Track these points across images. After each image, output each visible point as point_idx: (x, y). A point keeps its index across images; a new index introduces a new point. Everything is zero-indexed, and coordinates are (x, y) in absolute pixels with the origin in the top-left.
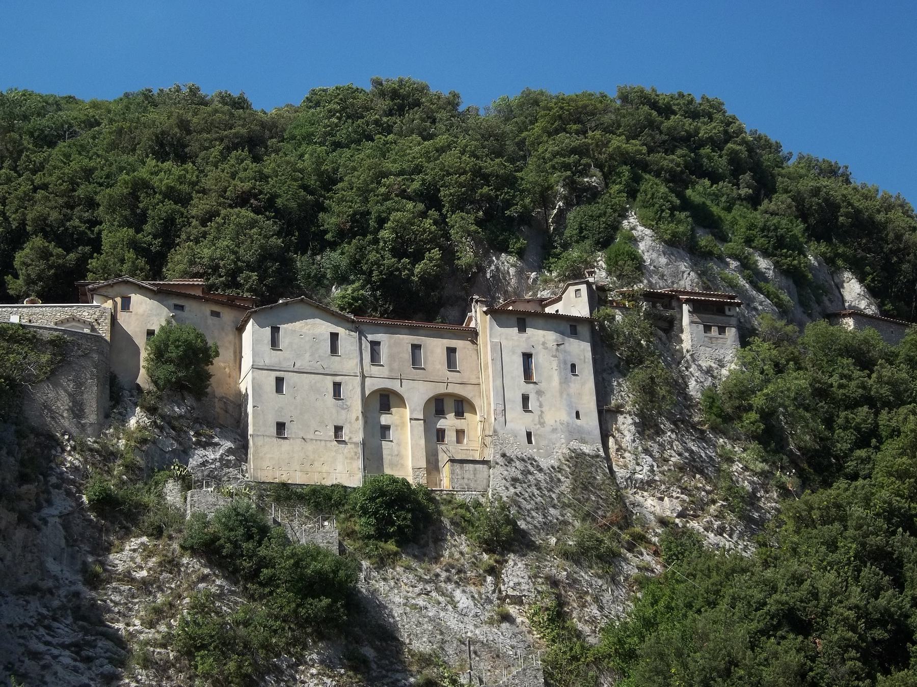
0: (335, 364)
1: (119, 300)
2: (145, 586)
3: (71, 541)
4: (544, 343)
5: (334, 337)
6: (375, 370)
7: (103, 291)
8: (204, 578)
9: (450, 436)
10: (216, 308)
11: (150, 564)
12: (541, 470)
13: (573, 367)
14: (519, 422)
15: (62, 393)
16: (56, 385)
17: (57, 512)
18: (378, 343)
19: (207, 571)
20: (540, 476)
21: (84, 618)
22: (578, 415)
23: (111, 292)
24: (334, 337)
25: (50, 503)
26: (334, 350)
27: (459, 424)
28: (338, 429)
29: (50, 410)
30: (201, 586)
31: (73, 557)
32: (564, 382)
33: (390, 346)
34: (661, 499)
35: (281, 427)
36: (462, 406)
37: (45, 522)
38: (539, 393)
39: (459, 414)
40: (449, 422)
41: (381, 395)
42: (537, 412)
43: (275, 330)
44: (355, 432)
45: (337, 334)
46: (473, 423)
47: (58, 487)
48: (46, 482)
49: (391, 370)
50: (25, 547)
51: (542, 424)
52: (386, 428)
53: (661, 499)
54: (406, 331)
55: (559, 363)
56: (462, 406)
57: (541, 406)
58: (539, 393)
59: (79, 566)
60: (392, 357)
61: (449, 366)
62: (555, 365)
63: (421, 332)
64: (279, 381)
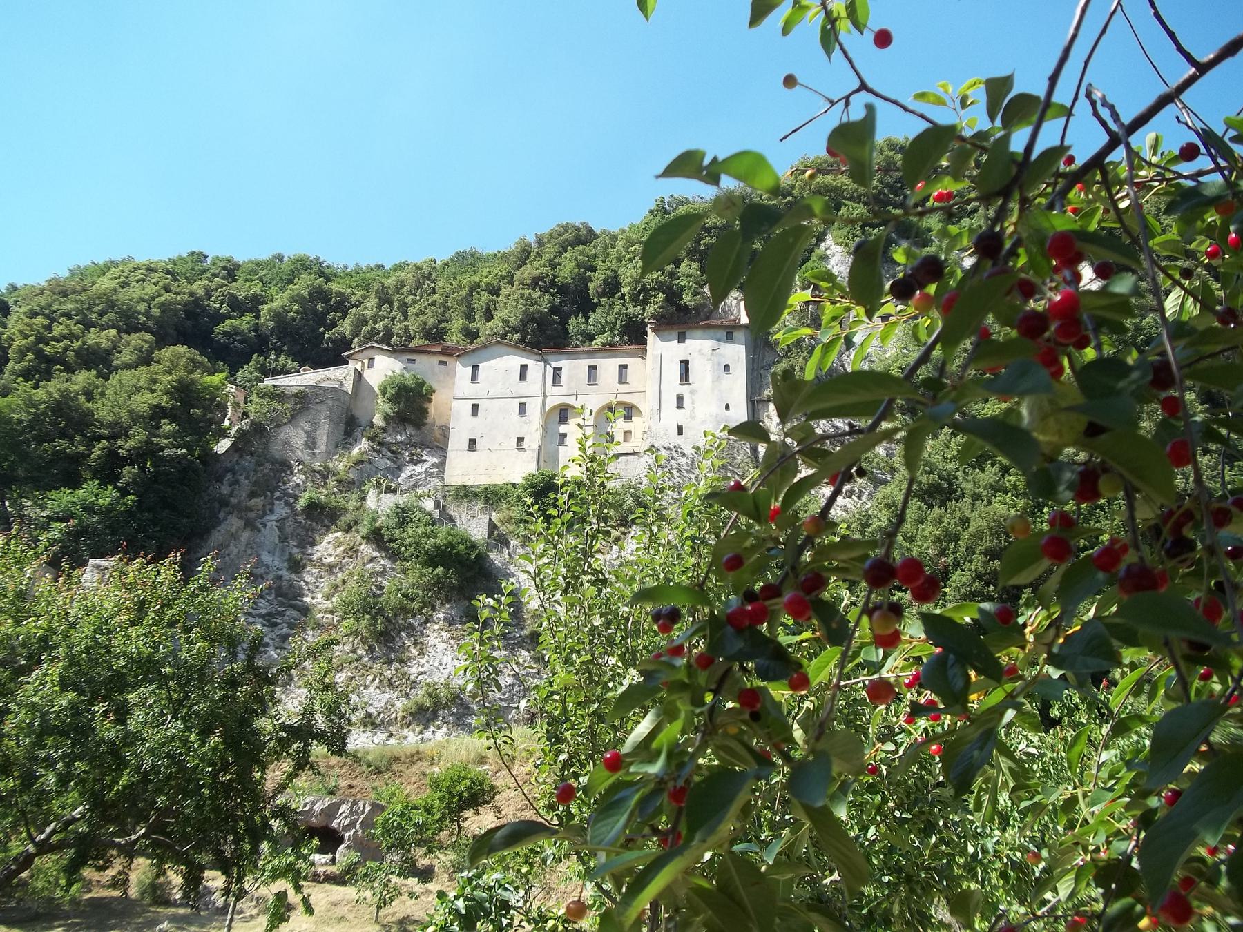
0: (523, 389)
1: (366, 361)
2: (331, 568)
3: (284, 539)
4: (700, 351)
5: (524, 368)
6: (556, 390)
7: (356, 356)
8: (372, 560)
10: (443, 359)
11: (338, 552)
12: (684, 455)
13: (727, 367)
14: (672, 416)
15: (301, 432)
16: (295, 427)
17: (275, 518)
18: (560, 369)
19: (375, 554)
20: (682, 461)
21: (285, 595)
22: (727, 407)
23: (360, 356)
24: (524, 368)
25: (272, 511)
26: (523, 377)
27: (627, 426)
28: (520, 440)
29: (289, 445)
30: (369, 566)
31: (283, 550)
32: (717, 380)
35: (472, 442)
36: (630, 411)
37: (265, 525)
38: (692, 392)
39: (628, 418)
41: (561, 410)
43: (475, 368)
44: (534, 440)
45: (526, 366)
46: (637, 424)
47: (279, 499)
48: (272, 496)
49: (569, 389)
51: (693, 418)
52: (565, 435)
54: (585, 356)
55: (713, 365)
56: (630, 411)
57: (693, 403)
58: (692, 392)
59: (287, 556)
61: (620, 379)
62: (709, 365)
63: (598, 355)
64: (475, 408)
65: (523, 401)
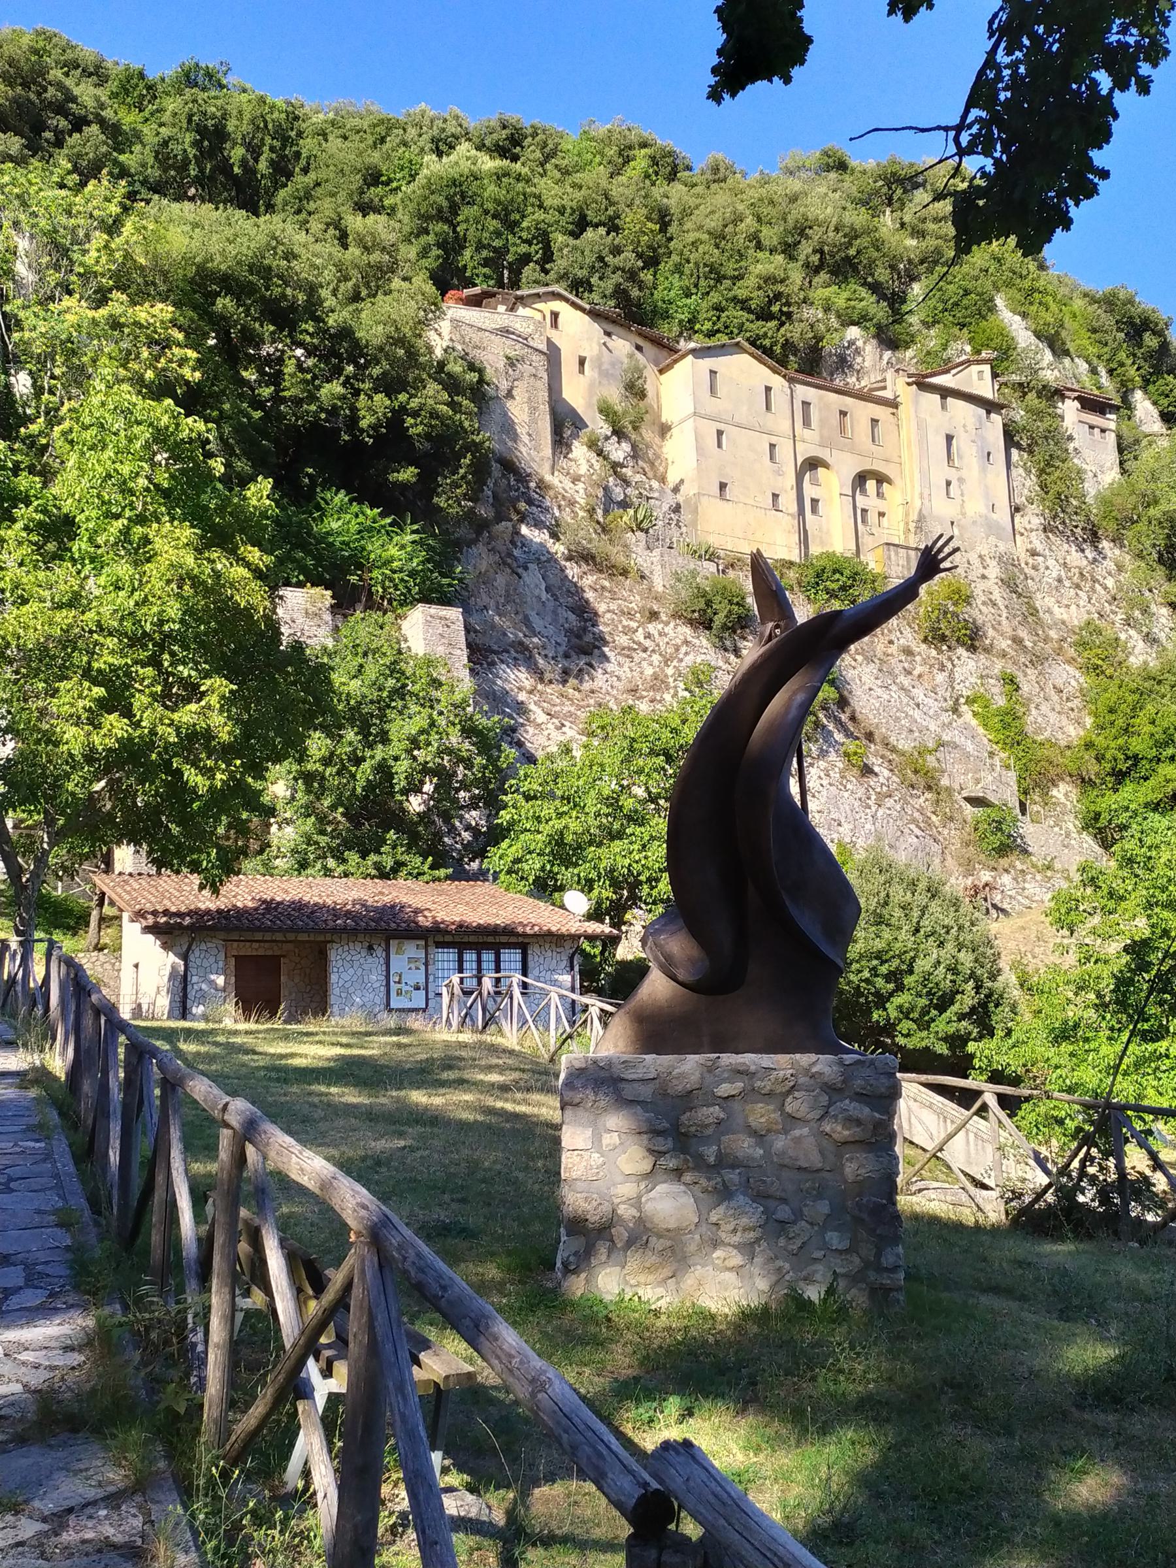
0: (769, 421)
9: (872, 517)
10: (640, 342)
27: (881, 505)
28: (775, 496)
32: (983, 470)
33: (820, 410)
34: (1068, 606)
35: (723, 486)
40: (869, 500)
42: (958, 500)
44: (788, 502)
49: (821, 437)
50: (507, 595)
51: (964, 514)
53: (1068, 606)
60: (823, 422)
62: (974, 450)
64: (720, 433)
65: (774, 440)
